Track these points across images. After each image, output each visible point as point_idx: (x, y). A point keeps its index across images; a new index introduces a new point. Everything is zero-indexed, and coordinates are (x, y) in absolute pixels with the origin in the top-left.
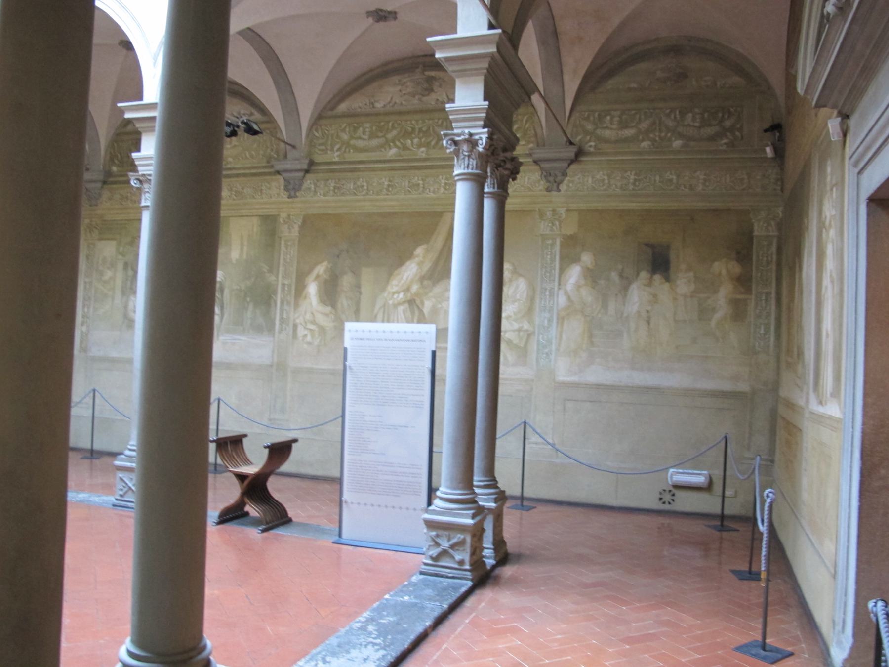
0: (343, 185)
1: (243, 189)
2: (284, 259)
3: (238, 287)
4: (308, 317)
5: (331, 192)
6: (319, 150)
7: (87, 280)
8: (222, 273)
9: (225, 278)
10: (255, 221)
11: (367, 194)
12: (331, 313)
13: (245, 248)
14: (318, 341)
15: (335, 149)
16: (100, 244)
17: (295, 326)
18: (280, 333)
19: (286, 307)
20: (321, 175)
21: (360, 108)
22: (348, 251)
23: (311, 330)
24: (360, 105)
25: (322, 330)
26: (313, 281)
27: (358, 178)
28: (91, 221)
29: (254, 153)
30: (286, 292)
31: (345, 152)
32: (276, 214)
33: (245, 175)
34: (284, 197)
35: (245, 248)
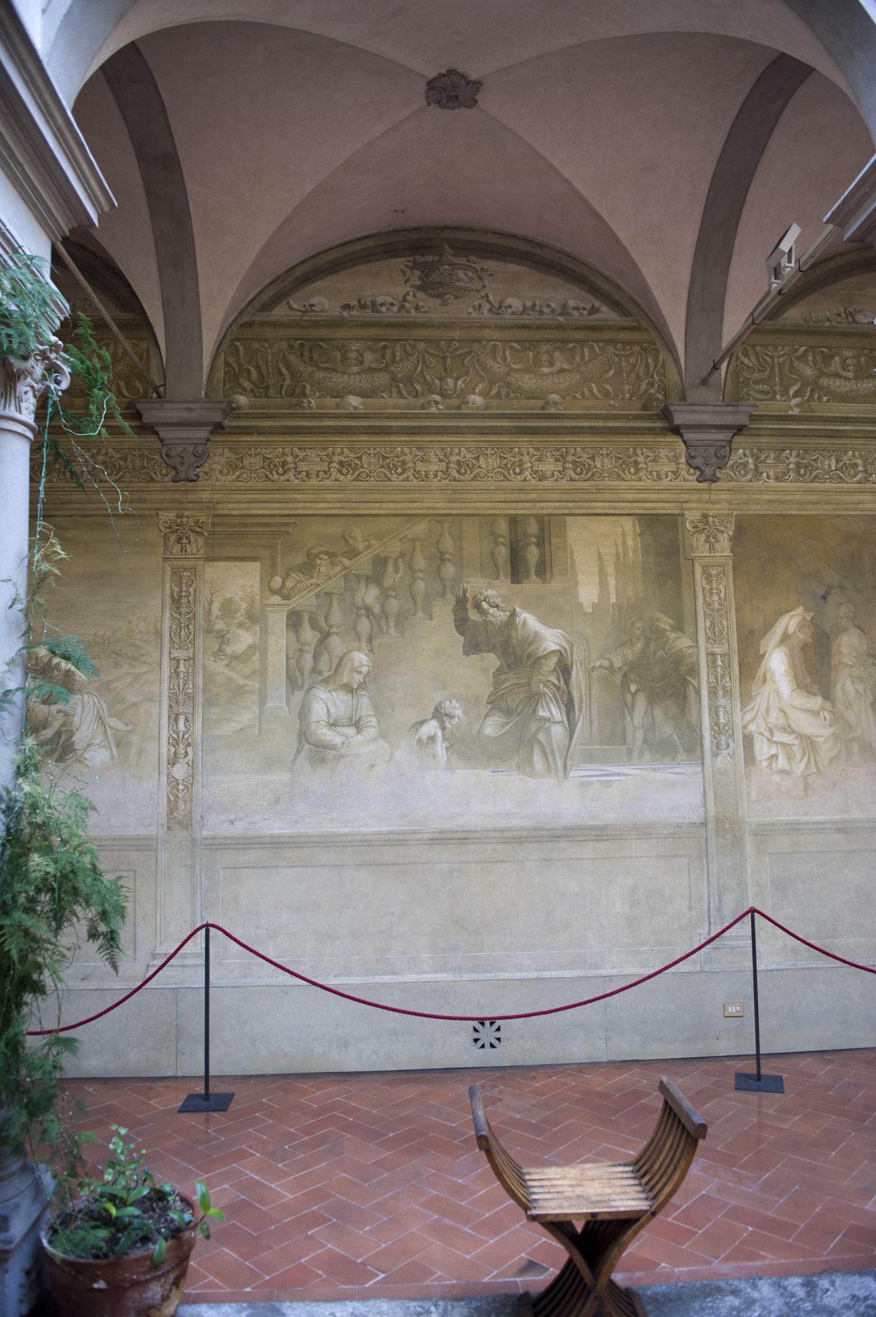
0: (816, 460)
1: (593, 458)
2: (708, 604)
3: (606, 663)
4: (775, 718)
5: (792, 475)
6: (760, 392)
7: (176, 654)
8: (561, 631)
9: (571, 645)
10: (628, 524)
11: (867, 480)
12: (822, 709)
13: (612, 581)
14: (803, 765)
15: (791, 392)
16: (213, 571)
17: (748, 740)
18: (715, 755)
19: (722, 701)
20: (765, 440)
21: (828, 320)
22: (842, 588)
23: (783, 744)
24: (828, 314)
25: (809, 743)
26: (778, 646)
27: (846, 452)
28: (179, 516)
29: (608, 387)
30: (719, 669)
31: (811, 398)
32: (677, 512)
33: (593, 431)
34: (690, 479)
35: (612, 581)
